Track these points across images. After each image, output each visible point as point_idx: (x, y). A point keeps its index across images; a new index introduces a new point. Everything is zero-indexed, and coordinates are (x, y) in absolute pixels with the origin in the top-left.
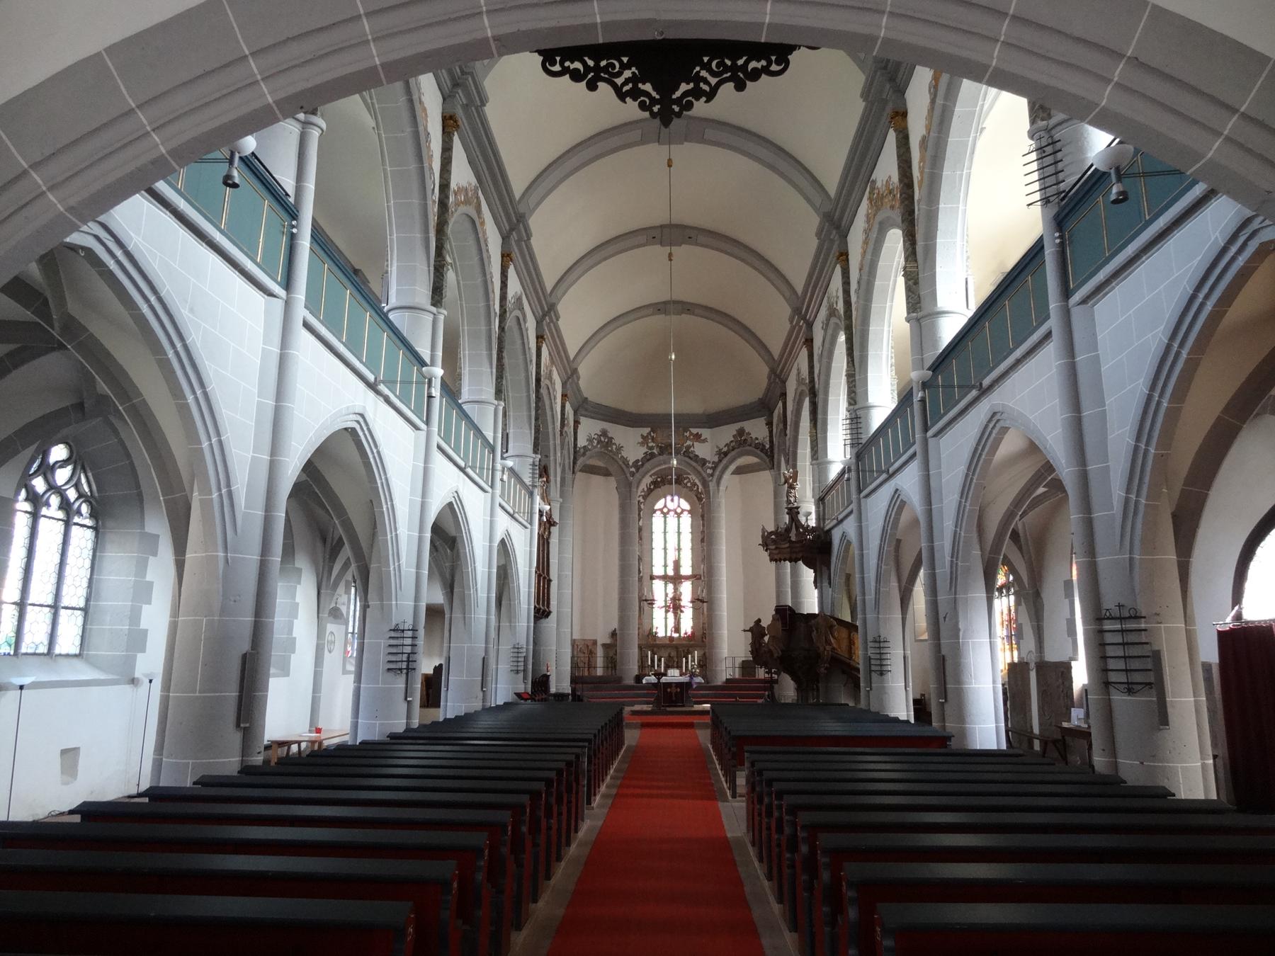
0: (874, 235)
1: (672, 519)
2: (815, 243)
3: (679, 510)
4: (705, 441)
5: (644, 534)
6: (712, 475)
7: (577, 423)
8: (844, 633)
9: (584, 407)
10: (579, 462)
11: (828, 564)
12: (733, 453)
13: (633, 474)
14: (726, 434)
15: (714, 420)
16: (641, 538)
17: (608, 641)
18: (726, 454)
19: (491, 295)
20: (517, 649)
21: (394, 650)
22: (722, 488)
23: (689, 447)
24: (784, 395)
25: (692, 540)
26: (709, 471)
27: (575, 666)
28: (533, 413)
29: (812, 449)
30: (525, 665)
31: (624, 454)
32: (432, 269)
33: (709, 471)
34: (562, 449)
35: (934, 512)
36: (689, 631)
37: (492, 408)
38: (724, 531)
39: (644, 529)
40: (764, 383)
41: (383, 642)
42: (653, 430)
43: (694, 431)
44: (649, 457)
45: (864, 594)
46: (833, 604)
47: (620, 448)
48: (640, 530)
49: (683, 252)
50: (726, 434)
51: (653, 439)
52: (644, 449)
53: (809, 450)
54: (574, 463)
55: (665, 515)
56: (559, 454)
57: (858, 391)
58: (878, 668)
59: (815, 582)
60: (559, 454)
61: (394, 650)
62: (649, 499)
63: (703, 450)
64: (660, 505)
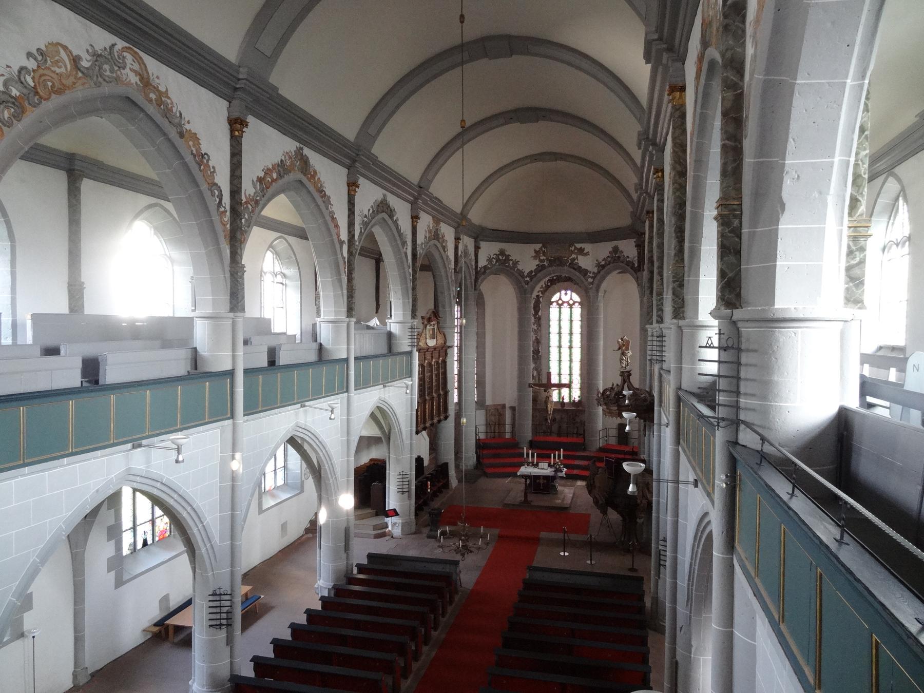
1: (566, 310)
3: (571, 302)
4: (587, 254)
5: (543, 322)
6: (592, 283)
7: (477, 248)
9: (480, 234)
13: (527, 283)
14: (602, 251)
15: (596, 237)
19: (334, 231)
21: (214, 610)
22: (601, 294)
23: (574, 259)
26: (590, 280)
28: (410, 285)
31: (520, 267)
32: (228, 275)
33: (590, 280)
36: (577, 399)
37: (345, 324)
39: (543, 318)
41: (206, 604)
42: (544, 246)
43: (578, 246)
44: (540, 268)
45: (658, 496)
47: (516, 263)
49: (543, 126)
50: (602, 251)
52: (537, 262)
55: (560, 306)
61: (214, 610)
62: (547, 294)
63: (585, 262)
64: (555, 298)
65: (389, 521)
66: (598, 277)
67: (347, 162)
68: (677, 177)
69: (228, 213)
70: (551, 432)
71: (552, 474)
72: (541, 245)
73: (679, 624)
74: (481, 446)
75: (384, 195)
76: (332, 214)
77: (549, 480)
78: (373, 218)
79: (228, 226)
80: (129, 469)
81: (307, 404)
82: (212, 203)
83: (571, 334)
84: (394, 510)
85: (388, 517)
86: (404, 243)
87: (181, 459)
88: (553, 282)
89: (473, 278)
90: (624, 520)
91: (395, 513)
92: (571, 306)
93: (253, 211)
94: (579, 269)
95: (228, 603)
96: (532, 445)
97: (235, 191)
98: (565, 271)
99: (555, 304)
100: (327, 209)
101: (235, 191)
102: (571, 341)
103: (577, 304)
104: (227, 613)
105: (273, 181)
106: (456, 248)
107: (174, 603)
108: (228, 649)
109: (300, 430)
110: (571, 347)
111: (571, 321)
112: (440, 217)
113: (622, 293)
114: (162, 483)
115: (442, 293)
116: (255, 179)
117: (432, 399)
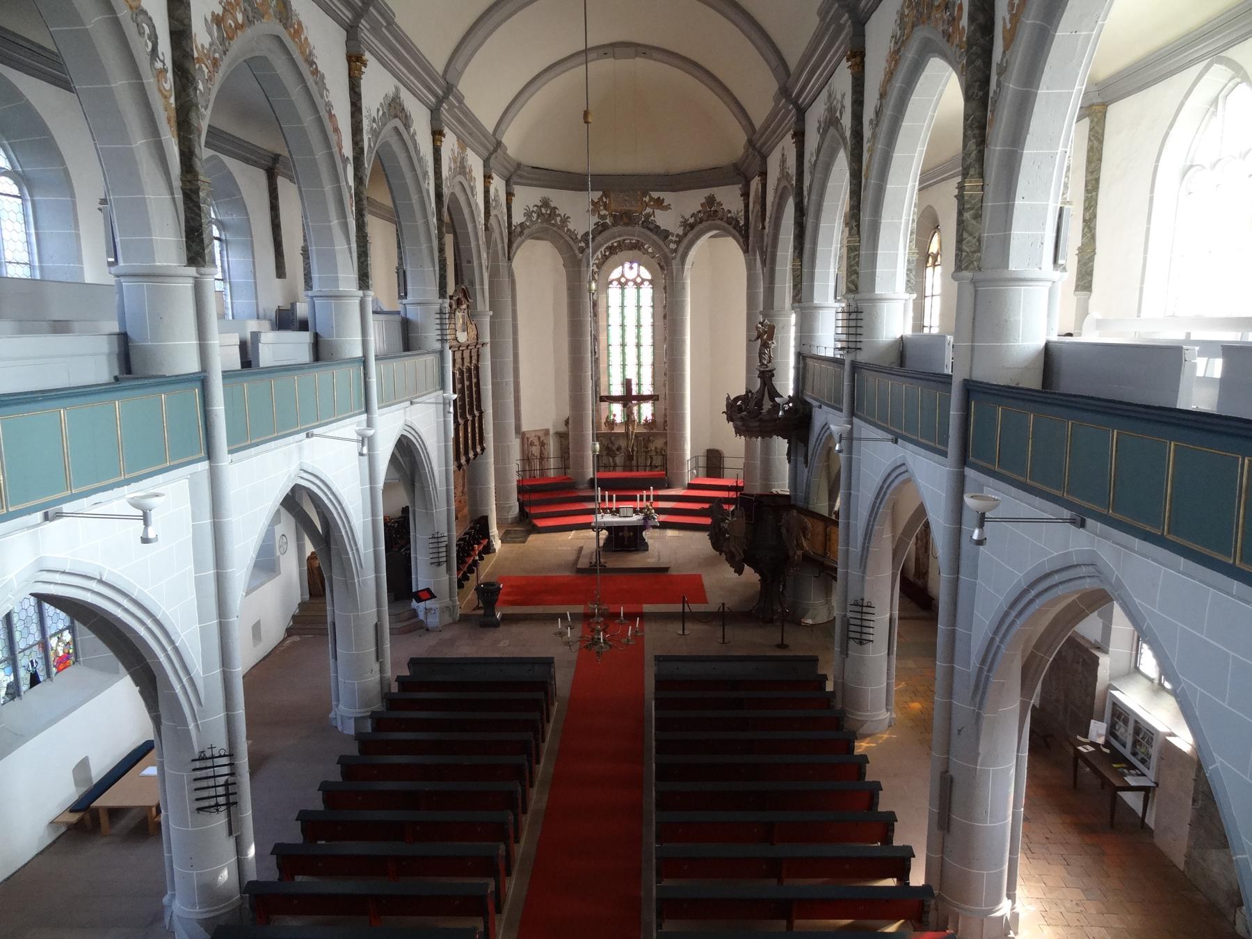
0: (910, 55)
1: (631, 290)
2: (814, 22)
3: (639, 280)
4: (668, 208)
5: (601, 310)
6: (675, 251)
7: (510, 195)
8: (820, 527)
10: (515, 246)
11: (805, 441)
12: (701, 226)
16: (595, 315)
17: (562, 429)
18: (692, 226)
19: (333, 138)
20: (436, 538)
22: (687, 266)
23: (648, 215)
24: (764, 174)
25: (653, 316)
26: (673, 246)
27: (526, 459)
28: (435, 243)
29: (795, 286)
30: (448, 556)
31: (571, 226)
32: (179, 196)
33: (673, 246)
34: (488, 248)
35: (962, 586)
36: (650, 418)
37: (357, 301)
38: (688, 299)
40: (740, 151)
41: (187, 776)
42: (605, 195)
43: (655, 195)
44: (601, 228)
45: (847, 544)
46: (808, 486)
47: (565, 220)
48: (595, 304)
51: (606, 206)
52: (595, 219)
53: (791, 250)
54: (510, 246)
55: (623, 286)
56: (484, 255)
57: (862, 271)
58: (858, 636)
59: (789, 454)
60: (484, 255)
62: (605, 268)
63: (667, 220)
64: (616, 274)
65: (420, 607)
66: (686, 241)
67: (347, 15)
68: (978, 35)
69: (170, 75)
70: (615, 466)
71: (641, 523)
72: (601, 193)
73: (956, 726)
74: (521, 490)
75: (397, 89)
76: (329, 106)
77: (637, 530)
78: (384, 125)
79: (172, 100)
80: (40, 560)
81: (316, 431)
82: (141, 48)
83: (639, 326)
84: (428, 590)
85: (419, 600)
86: (425, 174)
87: (151, 535)
88: (612, 250)
89: (506, 241)
90: (763, 580)
91: (429, 594)
92: (638, 286)
93: (210, 78)
94: (656, 230)
95: (226, 770)
96: (606, 485)
97: (180, 34)
98: (634, 233)
99: (615, 283)
100: (322, 96)
101: (180, 34)
102: (638, 336)
103: (646, 283)
104: (226, 785)
105: (239, 27)
106: (487, 192)
107: (98, 770)
108: (232, 841)
109: (305, 475)
110: (638, 346)
111: (639, 307)
112: (468, 139)
113: (716, 265)
114: (101, 582)
115: (469, 262)
116: (209, 18)
117: (466, 421)
